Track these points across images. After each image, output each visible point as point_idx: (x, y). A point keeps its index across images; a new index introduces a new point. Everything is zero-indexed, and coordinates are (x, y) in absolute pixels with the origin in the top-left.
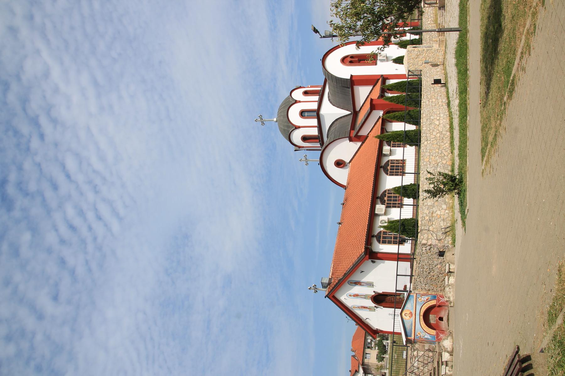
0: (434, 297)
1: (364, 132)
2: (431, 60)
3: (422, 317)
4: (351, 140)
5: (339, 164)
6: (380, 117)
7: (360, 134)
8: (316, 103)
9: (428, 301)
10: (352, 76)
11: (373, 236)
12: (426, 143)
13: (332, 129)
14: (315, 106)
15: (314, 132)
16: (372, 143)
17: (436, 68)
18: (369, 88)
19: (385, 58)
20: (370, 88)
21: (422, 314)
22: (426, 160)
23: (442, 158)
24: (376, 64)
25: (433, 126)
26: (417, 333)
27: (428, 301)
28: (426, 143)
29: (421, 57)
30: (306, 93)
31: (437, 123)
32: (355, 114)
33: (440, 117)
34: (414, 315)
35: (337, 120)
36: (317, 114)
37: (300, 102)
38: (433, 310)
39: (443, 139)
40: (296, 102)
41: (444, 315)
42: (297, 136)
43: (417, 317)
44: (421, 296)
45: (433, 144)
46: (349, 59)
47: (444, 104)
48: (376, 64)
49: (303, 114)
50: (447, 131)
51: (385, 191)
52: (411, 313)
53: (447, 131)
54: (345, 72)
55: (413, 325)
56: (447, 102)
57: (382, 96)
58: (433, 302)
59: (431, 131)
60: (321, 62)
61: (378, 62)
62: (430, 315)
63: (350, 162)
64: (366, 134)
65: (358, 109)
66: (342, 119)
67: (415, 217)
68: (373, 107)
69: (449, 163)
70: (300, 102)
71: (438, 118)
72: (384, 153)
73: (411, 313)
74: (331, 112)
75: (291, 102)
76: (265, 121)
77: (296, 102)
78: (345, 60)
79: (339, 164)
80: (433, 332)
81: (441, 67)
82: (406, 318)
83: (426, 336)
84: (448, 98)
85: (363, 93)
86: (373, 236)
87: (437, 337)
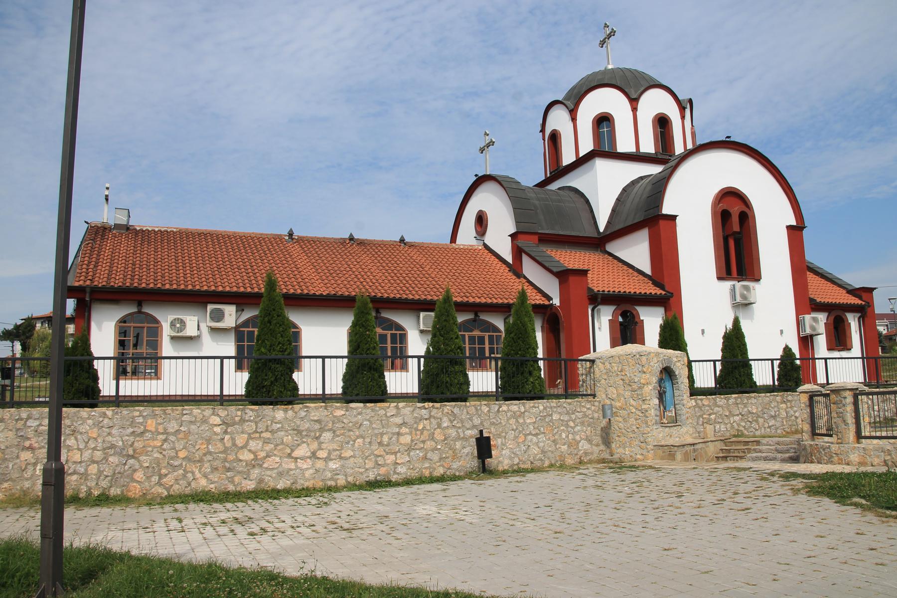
1: (529, 268)
2: (618, 424)
4: (513, 236)
5: (481, 220)
6: (549, 298)
7: (526, 260)
8: (632, 149)
10: (673, 218)
11: (140, 304)
12: (216, 420)
13: (572, 194)
14: (625, 145)
15: (568, 158)
16: (506, 289)
17: (597, 439)
18: (646, 267)
19: (739, 299)
20: (647, 269)
22: (151, 424)
23: (154, 469)
24: (720, 278)
25: (288, 439)
28: (216, 420)
29: (628, 394)
30: (662, 123)
31: (302, 451)
32: (598, 243)
33: (327, 459)
35: (587, 201)
36: (604, 150)
37: (634, 110)
39: (229, 470)
40: (634, 102)
42: (559, 120)
45: (208, 441)
46: (736, 210)
47: (383, 471)
48: (720, 278)
49: (603, 121)
50: (261, 481)
51: (295, 326)
53: (261, 481)
54: (690, 200)
56: (394, 478)
57: (598, 299)
59: (267, 435)
60: (722, 138)
61: (728, 284)
63: (485, 246)
64: (526, 272)
65: (611, 247)
66: (585, 215)
67: (101, 399)
68: (563, 275)
69: (135, 490)
70: (634, 110)
71: (322, 454)
72: (422, 314)
74: (605, 186)
75: (633, 85)
76: (607, 47)
77: (634, 102)
78: (731, 200)
79: (481, 220)
81: (597, 450)
84: (421, 480)
85: (636, 251)
86: (140, 304)
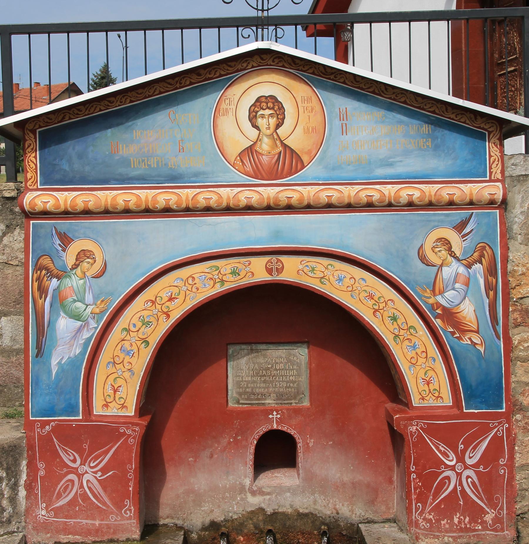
0: (482, 389)
3: (257, 272)
9: (442, 323)
21: (292, 271)
26: (86, 238)
27: (442, 323)
34: (269, 193)
38: (355, 376)
41: (324, 487)
43: (257, 230)
44: (479, 254)
52: (290, 162)
55: (163, 198)
58: (426, 379)
62: (301, 354)
73: (290, 162)
80: (118, 393)
82: (231, 119)
83: (64, 325)
87: (69, 435)
